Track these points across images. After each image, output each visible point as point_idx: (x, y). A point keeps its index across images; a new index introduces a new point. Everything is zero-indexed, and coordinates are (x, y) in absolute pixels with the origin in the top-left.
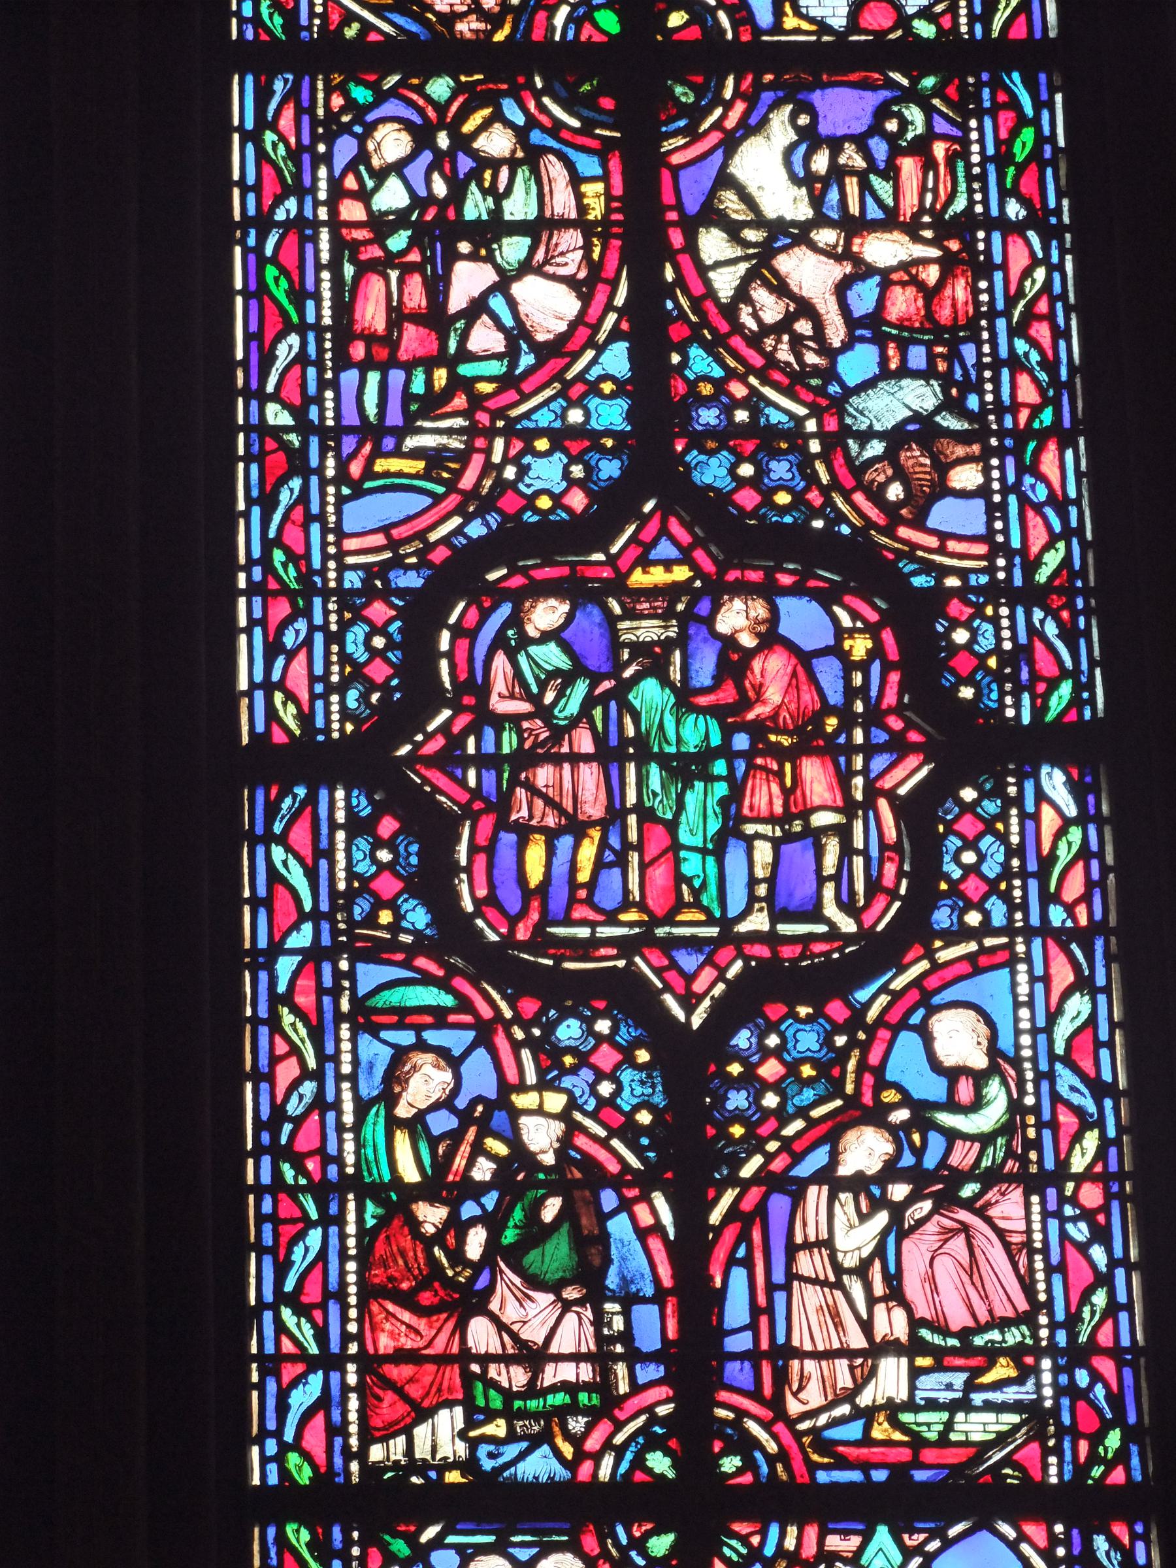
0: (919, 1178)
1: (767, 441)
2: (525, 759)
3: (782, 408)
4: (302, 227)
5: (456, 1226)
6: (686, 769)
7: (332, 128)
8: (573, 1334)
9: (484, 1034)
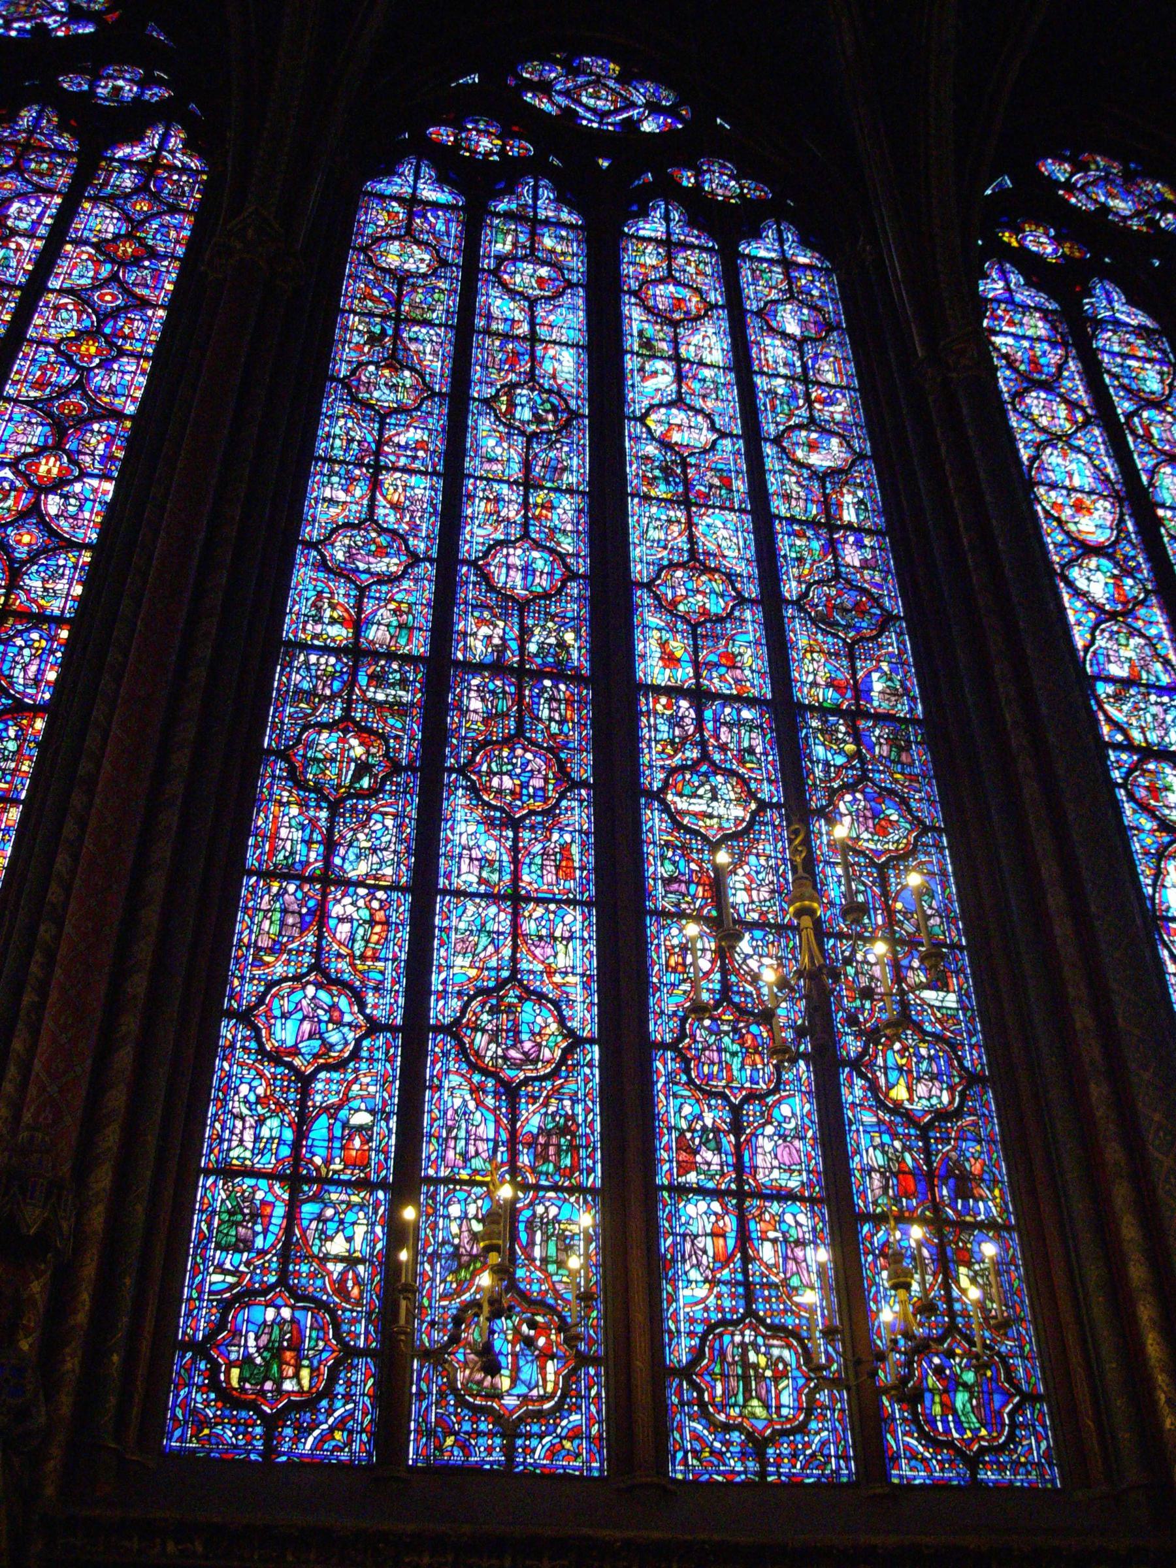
0: (780, 1136)
1: (747, 994)
2: (704, 1049)
3: (749, 988)
4: (658, 945)
5: (693, 1138)
7: (664, 927)
8: (716, 1160)
9: (698, 1101)
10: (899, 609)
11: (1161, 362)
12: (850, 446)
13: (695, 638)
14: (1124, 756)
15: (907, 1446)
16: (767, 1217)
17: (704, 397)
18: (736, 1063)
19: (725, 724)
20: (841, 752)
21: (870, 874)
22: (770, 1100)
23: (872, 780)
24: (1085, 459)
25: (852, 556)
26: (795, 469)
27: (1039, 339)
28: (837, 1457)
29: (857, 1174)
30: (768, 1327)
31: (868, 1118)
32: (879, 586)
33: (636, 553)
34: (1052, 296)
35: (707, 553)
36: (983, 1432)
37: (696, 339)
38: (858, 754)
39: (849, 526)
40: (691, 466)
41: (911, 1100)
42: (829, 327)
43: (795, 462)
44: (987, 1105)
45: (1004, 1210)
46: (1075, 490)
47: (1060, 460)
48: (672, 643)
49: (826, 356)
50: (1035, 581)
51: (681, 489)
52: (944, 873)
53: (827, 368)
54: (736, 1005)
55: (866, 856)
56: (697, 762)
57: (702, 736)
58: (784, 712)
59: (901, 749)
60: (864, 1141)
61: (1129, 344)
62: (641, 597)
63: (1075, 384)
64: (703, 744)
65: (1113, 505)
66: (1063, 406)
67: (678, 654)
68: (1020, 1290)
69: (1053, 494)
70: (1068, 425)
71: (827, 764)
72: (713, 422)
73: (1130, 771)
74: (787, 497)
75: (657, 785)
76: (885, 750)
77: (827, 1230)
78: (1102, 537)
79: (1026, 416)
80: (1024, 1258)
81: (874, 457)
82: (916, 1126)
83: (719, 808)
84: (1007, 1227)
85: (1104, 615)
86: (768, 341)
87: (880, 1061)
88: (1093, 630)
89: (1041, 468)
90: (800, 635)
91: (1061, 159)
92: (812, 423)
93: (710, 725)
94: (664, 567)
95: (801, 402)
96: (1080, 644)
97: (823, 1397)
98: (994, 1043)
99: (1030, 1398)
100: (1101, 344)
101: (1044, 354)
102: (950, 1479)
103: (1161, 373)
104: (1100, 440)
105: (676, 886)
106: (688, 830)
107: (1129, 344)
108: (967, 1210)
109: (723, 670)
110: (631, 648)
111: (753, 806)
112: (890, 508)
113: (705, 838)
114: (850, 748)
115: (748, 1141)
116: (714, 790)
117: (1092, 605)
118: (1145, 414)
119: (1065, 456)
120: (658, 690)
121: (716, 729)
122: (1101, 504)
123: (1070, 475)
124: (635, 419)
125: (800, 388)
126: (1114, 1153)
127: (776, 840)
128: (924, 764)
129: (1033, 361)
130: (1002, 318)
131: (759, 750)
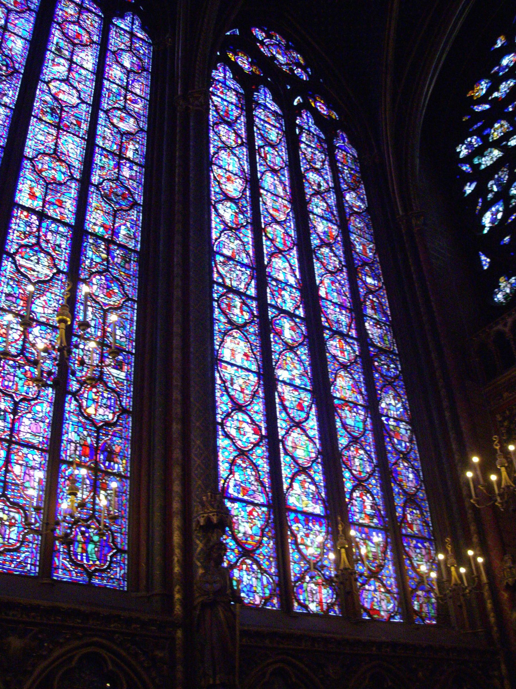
2: (8, 374)
6: (21, 379)
10: (141, 201)
11: (279, 129)
12: (138, 124)
13: (47, 188)
14: (220, 289)
15: (63, 564)
16: (20, 454)
17: (79, 82)
18: (21, 383)
19: (51, 231)
20: (99, 256)
21: (100, 313)
22: (33, 403)
23: (110, 272)
24: (237, 160)
25: (126, 172)
26: (111, 126)
27: (232, 103)
28: (31, 564)
29: (65, 442)
30: (11, 503)
31: (75, 419)
32: (135, 189)
33: (29, 143)
34: (242, 87)
35: (62, 153)
36: (98, 563)
37: (83, 55)
38: (107, 260)
39: (128, 159)
40: (65, 111)
41: (95, 415)
42: (144, 69)
43: (112, 124)
44: (128, 423)
45: (126, 470)
46: (229, 171)
47: (226, 157)
48: (35, 189)
49: (139, 81)
50: (202, 205)
51: (57, 120)
52: (132, 320)
53: (137, 86)
54: (26, 357)
55: (100, 305)
56: (34, 245)
57: (39, 234)
58: (79, 233)
59: (126, 262)
60: (71, 428)
61: (268, 117)
62: (26, 164)
63: (241, 127)
64: (38, 237)
65: (243, 182)
66: (234, 135)
67: (38, 194)
68: (126, 505)
69: (220, 171)
70: (233, 143)
71: (92, 259)
72: (80, 95)
73: (222, 295)
74: (104, 138)
75: (12, 251)
76: (119, 261)
77: (46, 465)
78: (235, 194)
79: (217, 134)
80: (130, 492)
81: (148, 132)
82: (95, 426)
83: (38, 268)
84: (126, 477)
85: (227, 228)
86: (114, 66)
87: (85, 395)
88: (221, 232)
89: (217, 158)
90: (94, 200)
91: (262, 31)
92: (124, 109)
93: (44, 230)
94: (40, 153)
95: (122, 98)
96: (214, 237)
97: (30, 537)
98: (137, 397)
99: (121, 551)
100: (257, 113)
101: (232, 110)
102: (79, 581)
103: (278, 134)
104: (245, 153)
105: (11, 298)
106: (22, 274)
107: (268, 117)
108: (109, 467)
109: (55, 207)
110: (16, 186)
111: (55, 271)
112: (147, 157)
113: (29, 280)
114: (104, 256)
115: (19, 419)
116: (39, 259)
117: (223, 222)
118: (267, 149)
119: (229, 156)
120: (24, 208)
121: (46, 232)
122: (238, 180)
123: (229, 164)
124: (45, 82)
125: (123, 92)
126: (177, 454)
127: (62, 288)
128: (136, 271)
129: (227, 112)
130: (218, 89)
131: (63, 246)
